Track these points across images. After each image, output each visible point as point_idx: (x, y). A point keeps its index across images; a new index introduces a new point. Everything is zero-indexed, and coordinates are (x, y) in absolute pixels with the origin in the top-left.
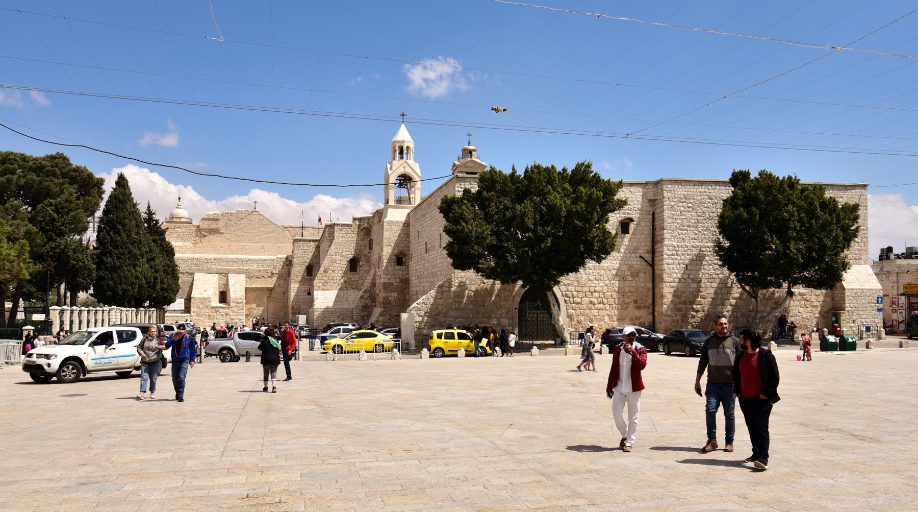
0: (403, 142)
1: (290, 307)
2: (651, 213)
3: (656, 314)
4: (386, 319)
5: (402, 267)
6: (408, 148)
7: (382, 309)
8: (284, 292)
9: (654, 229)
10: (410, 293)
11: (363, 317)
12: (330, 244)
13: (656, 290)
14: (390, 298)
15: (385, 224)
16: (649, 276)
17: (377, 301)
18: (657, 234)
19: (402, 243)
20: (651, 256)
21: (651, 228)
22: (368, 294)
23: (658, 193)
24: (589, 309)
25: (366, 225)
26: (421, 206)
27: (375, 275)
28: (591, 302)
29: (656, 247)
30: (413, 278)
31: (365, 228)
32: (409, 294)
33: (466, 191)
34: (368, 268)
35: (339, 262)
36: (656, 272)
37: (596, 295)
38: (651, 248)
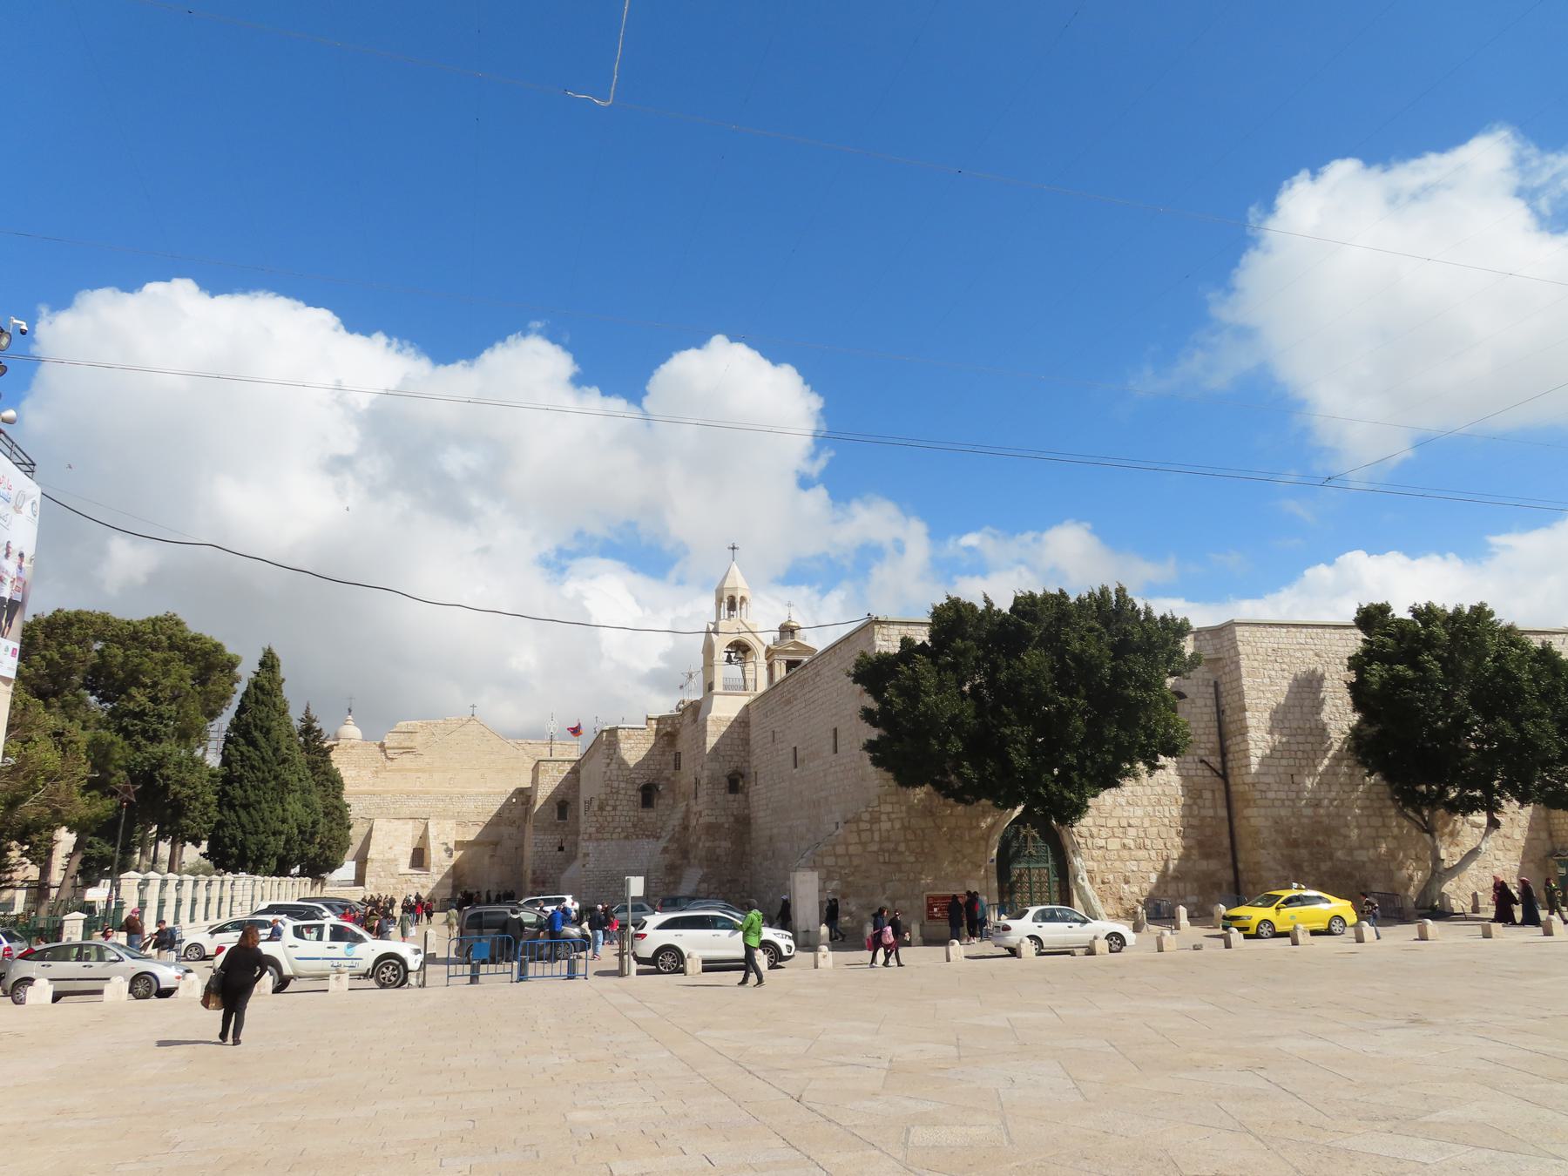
0: (736, 589)
1: (529, 872)
2: (1212, 683)
3: (1241, 866)
4: (712, 887)
5: (737, 796)
6: (743, 599)
7: (705, 870)
8: (516, 848)
9: (1220, 712)
10: (752, 842)
11: (668, 884)
12: (608, 761)
13: (1236, 823)
14: (718, 850)
15: (709, 723)
16: (1220, 795)
17: (691, 856)
18: (1228, 720)
19: (737, 755)
20: (1219, 759)
21: (1215, 709)
22: (676, 845)
23: (1222, 647)
24: (1121, 859)
25: (669, 729)
26: (780, 688)
27: (688, 811)
28: (1124, 846)
29: (1228, 743)
30: (761, 814)
31: (667, 734)
32: (750, 843)
33: (906, 642)
34: (671, 802)
35: (623, 792)
36: (1233, 788)
37: (1132, 832)
38: (1217, 746)
